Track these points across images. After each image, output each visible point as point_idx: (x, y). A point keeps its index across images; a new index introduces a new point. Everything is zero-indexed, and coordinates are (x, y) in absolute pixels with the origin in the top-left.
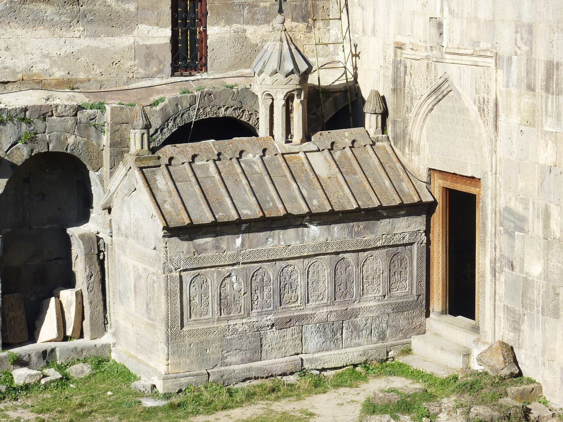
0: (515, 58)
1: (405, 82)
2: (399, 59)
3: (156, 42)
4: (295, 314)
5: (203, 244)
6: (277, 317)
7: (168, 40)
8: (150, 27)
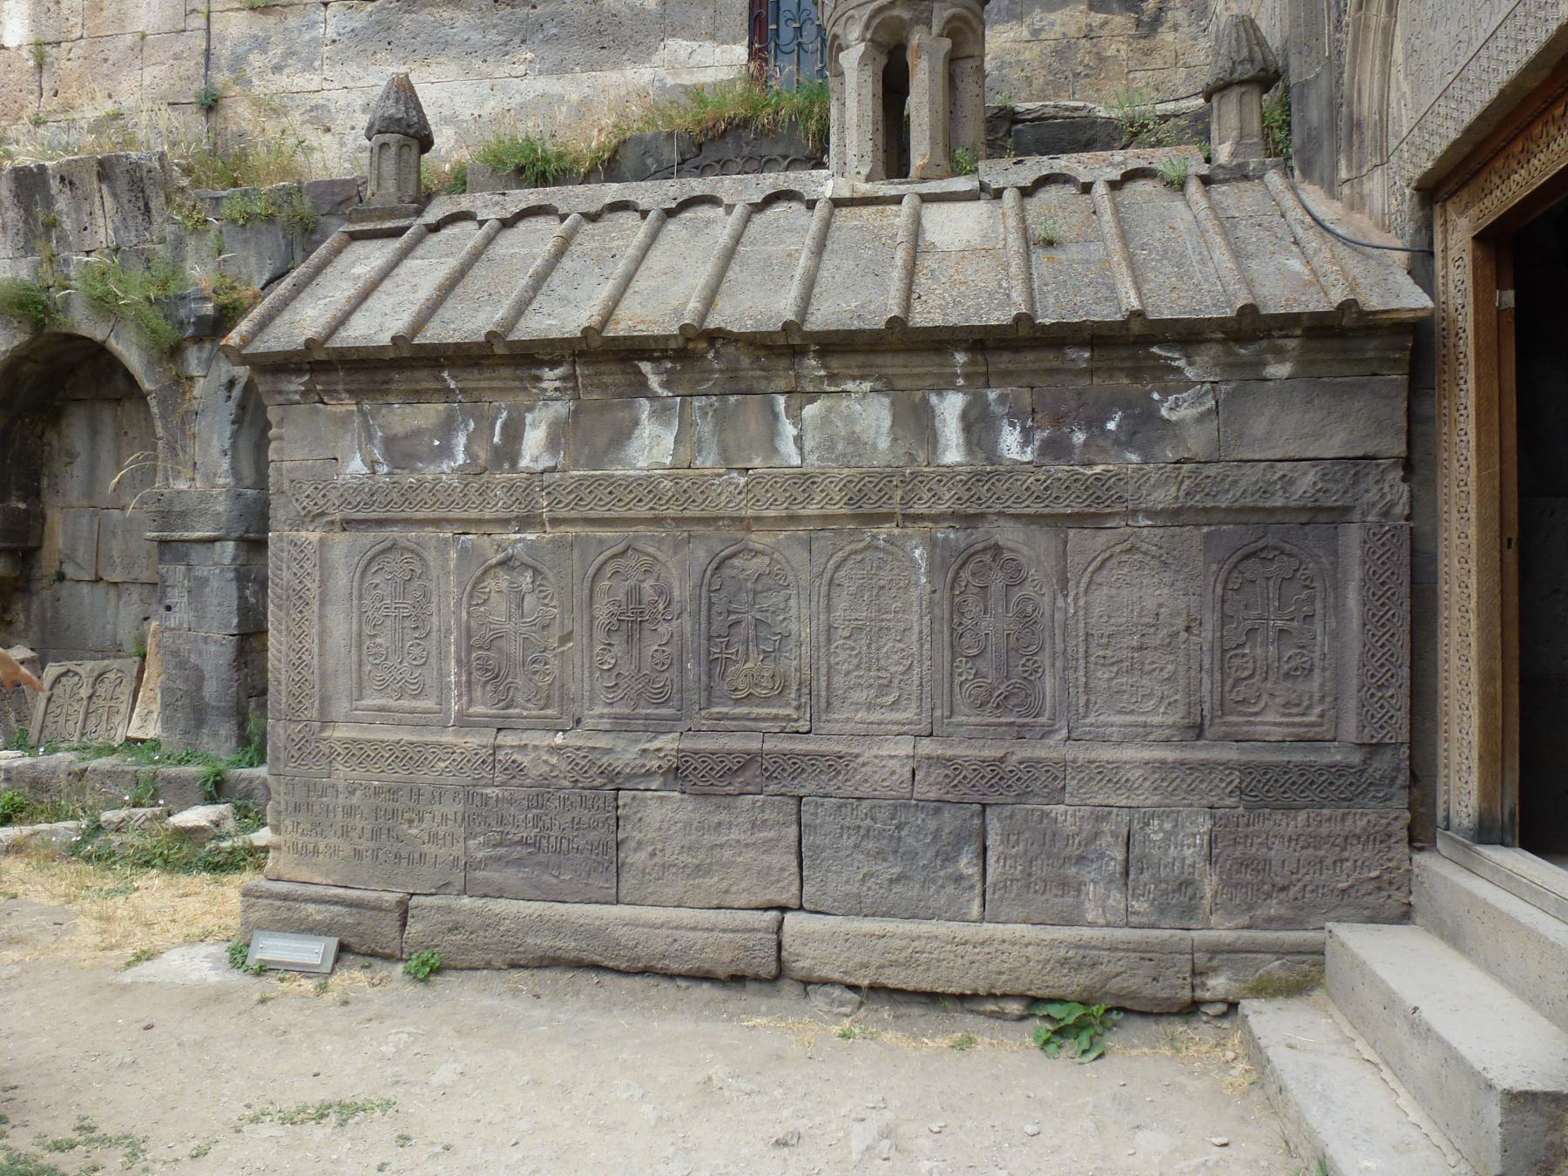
3: (708, 77)
4: (768, 746)
5: (406, 437)
6: (688, 744)
8: (695, 44)
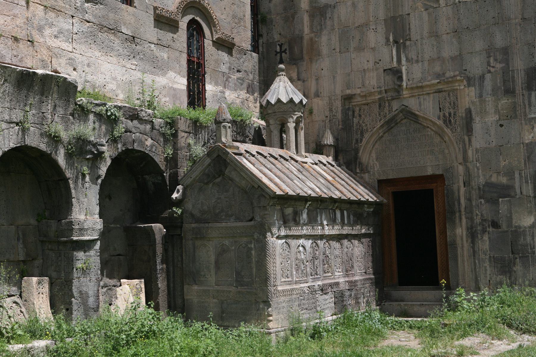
0: (488, 76)
1: (353, 122)
2: (347, 107)
7: (185, 88)
